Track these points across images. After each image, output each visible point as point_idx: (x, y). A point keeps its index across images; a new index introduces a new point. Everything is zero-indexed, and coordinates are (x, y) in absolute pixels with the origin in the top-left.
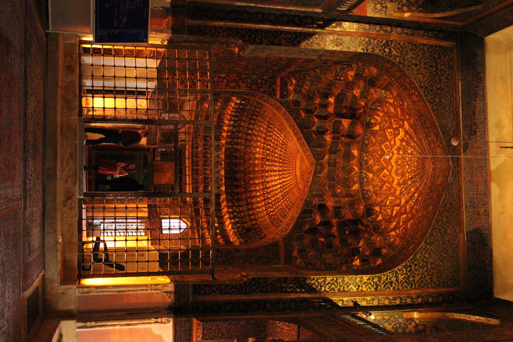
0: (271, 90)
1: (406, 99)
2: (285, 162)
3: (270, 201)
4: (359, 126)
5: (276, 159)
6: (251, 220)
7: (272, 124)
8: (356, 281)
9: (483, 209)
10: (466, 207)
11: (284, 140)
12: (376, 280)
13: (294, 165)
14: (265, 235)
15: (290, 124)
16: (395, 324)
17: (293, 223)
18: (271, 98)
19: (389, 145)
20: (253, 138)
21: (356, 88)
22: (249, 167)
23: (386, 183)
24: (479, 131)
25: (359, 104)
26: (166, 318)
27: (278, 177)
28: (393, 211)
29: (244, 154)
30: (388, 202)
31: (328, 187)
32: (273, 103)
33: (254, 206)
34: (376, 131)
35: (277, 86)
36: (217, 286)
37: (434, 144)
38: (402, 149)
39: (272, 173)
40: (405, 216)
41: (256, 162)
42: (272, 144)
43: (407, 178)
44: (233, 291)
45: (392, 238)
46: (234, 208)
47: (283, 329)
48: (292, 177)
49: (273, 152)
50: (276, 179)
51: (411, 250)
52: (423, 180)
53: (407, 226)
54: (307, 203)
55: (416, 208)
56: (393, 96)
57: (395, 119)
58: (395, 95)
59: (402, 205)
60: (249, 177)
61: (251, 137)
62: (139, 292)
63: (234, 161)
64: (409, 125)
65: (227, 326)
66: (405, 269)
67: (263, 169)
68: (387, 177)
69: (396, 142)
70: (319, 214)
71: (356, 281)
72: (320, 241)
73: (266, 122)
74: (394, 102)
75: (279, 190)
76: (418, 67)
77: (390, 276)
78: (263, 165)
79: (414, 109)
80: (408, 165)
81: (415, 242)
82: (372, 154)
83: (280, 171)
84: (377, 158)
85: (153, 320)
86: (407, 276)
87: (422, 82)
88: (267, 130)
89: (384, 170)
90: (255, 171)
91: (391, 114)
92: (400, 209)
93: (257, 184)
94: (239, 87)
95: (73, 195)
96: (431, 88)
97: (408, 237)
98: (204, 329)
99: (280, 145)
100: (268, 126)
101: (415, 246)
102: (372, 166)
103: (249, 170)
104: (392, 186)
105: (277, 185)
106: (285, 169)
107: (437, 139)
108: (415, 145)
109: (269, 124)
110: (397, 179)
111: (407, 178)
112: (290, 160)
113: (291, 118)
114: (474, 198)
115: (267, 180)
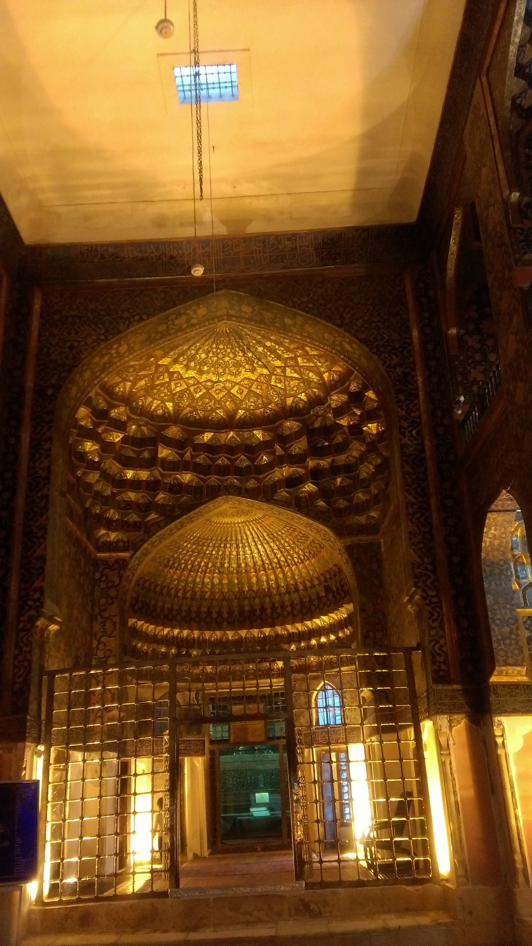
0: (116, 566)
1: (126, 362)
2: (224, 538)
3: (283, 559)
4: (168, 433)
5: (220, 553)
6: (313, 586)
7: (169, 561)
8: (406, 426)
9: (287, 242)
10: (284, 268)
11: (192, 541)
12: (402, 397)
13: (229, 525)
14: (335, 565)
15: (168, 534)
16: (469, 365)
17: (316, 524)
18: (130, 566)
19: (195, 387)
20: (189, 589)
21: (111, 438)
23: (252, 389)
24: (170, 251)
25: (136, 431)
26: (495, 728)
27: (247, 548)
28: (292, 378)
29: (214, 601)
30: (279, 385)
31: (259, 474)
32: (137, 562)
33: (291, 582)
34: (174, 407)
35: (111, 557)
36: (433, 643)
37: (192, 318)
38: (200, 367)
39: (242, 557)
40: (299, 359)
41: (225, 581)
42: (199, 560)
43: (243, 358)
44: (439, 616)
45: (333, 377)
46: (295, 612)
47: (494, 536)
48: (247, 528)
49: (209, 558)
50: (249, 552)
51: (352, 347)
52: (247, 334)
53: (314, 355)
54: (285, 504)
55: (288, 343)
56: (121, 382)
57: (156, 379)
58: (120, 380)
59: (283, 365)
60: (247, 592)
61: (187, 592)
62: (455, 776)
64: (164, 357)
65: (497, 625)
66: (384, 355)
67: (235, 571)
68: (243, 388)
69: (191, 376)
70: (301, 486)
71: (406, 426)
72: (342, 482)
73: (166, 570)
74: (130, 381)
75: (266, 546)
76: (76, 344)
77: (395, 377)
78: (229, 572)
79: (140, 349)
80: (223, 357)
81: (341, 342)
82: (208, 411)
83: (238, 547)
84: (214, 403)
85: (500, 751)
86: (394, 351)
87: (98, 338)
88: (177, 569)
89: (232, 394)
90: (238, 584)
91: (149, 384)
92: (289, 367)
94: (113, 616)
95: (302, 900)
96: (107, 324)
97: (332, 352)
98: (507, 664)
99: (199, 548)
100: (171, 568)
101: (345, 341)
102: (227, 411)
104: (256, 380)
105: (258, 549)
106: (234, 538)
107: (184, 314)
108: (193, 348)
109: (168, 565)
110: (245, 374)
111: (243, 358)
112: (220, 531)
113: (158, 534)
114: (270, 257)
115: (251, 564)
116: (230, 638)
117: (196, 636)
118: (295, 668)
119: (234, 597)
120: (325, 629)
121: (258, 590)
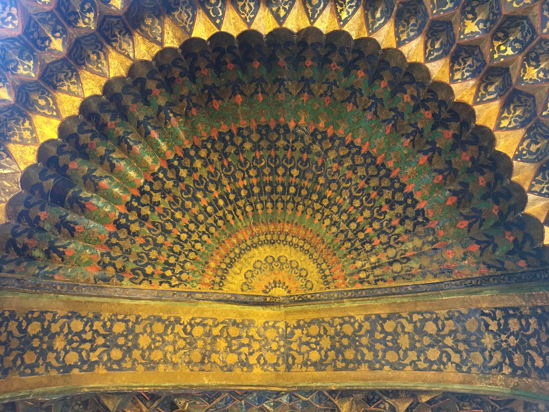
22: (287, 90)
29: (332, 81)
67: (282, 131)
119: (285, 83)
121: (234, 94)
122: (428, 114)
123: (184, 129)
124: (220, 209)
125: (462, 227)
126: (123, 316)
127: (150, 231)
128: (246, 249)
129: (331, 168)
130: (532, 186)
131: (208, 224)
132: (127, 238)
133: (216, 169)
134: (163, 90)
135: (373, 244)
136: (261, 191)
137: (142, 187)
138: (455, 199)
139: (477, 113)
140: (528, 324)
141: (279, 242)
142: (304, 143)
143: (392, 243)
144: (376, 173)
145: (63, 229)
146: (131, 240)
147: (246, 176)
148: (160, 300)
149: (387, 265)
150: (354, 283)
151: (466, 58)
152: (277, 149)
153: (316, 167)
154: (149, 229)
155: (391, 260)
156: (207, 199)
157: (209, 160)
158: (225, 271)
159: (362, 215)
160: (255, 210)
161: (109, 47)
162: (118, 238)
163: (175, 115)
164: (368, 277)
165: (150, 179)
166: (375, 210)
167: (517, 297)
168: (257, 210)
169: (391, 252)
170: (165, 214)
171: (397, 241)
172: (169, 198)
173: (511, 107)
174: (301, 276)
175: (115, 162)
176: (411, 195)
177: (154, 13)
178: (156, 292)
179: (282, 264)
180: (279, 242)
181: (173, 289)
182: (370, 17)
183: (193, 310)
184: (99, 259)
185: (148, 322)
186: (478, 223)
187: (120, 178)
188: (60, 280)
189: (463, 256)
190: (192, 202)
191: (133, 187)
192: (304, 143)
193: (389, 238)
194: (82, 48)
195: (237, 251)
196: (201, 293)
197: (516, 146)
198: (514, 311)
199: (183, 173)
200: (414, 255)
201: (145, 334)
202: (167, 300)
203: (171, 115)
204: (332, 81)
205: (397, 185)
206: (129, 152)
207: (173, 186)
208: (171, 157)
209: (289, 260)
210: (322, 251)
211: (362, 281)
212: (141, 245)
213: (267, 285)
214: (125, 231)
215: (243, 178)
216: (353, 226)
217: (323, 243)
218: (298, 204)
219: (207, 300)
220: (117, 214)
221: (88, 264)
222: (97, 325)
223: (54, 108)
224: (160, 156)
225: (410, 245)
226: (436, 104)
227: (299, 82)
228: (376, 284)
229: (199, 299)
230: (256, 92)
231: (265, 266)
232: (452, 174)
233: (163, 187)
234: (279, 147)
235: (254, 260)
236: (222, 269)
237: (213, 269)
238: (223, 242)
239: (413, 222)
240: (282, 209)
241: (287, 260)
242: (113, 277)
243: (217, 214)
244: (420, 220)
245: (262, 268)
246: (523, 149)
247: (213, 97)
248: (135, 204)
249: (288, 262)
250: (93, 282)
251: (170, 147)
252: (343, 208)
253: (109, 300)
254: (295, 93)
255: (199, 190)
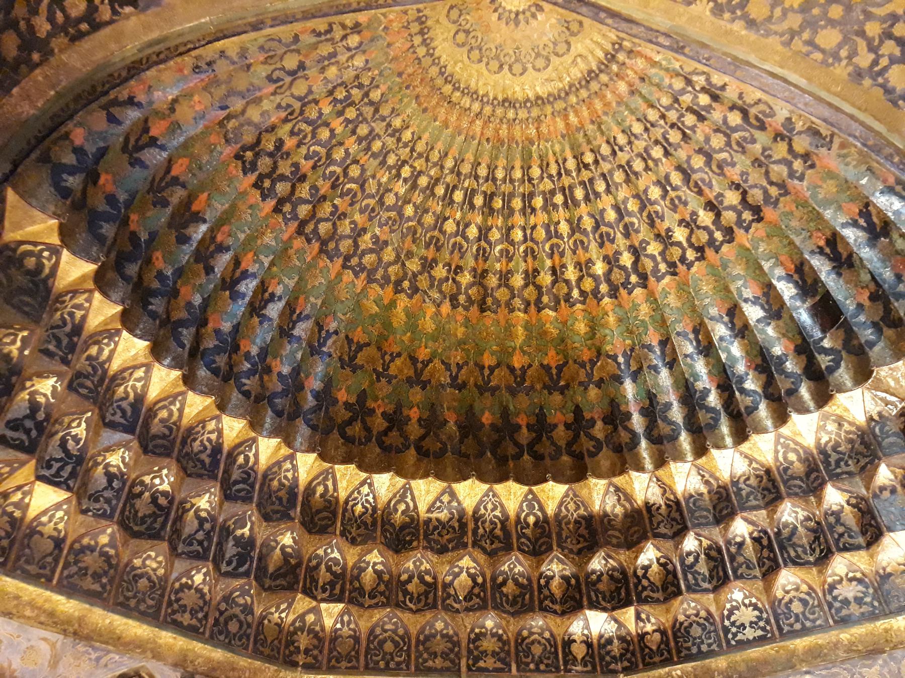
22: (448, 366)
61: (300, 318)
63: (414, 430)
93: (537, 333)
103: (459, 367)
116: (422, 508)
117: (304, 477)
118: (657, 636)
119: (449, 380)
120: (793, 478)
121: (524, 370)
122: (245, 346)
123: (607, 331)
124: (582, 183)
125: (180, 161)
126: (812, 56)
127: (710, 181)
128: (555, 99)
129: (392, 231)
130: (89, 300)
131: (610, 162)
132: (751, 187)
133: (574, 253)
134: (623, 408)
135: (331, 99)
136: (509, 201)
137: (697, 259)
138: (195, 208)
139: (181, 382)
140: (51, 19)
141: (496, 102)
142: (431, 276)
143: (297, 105)
144: (320, 226)
145: (844, 256)
146: (746, 181)
147: (528, 232)
148: (735, 58)
149: (308, 63)
150: (370, 22)
151: (201, 452)
152: (474, 270)
153: (415, 233)
154: (711, 187)
155: (300, 74)
156: (601, 207)
157: (581, 270)
158: (603, 67)
159: (347, 151)
160: (526, 168)
161: (680, 496)
162: (766, 192)
163: (614, 358)
164: (345, 37)
165: (681, 268)
166: (323, 160)
167: (78, 65)
168: (522, 167)
169: (300, 88)
170: (677, 202)
171: (289, 110)
172: (662, 226)
173: (132, 395)
174: (467, 32)
175: (726, 319)
176: (264, 197)
177: (610, 521)
178: (738, 73)
179: (497, 57)
180: (496, 102)
181: (706, 69)
182: (331, 487)
183: (684, 19)
184: (810, 171)
185: (773, 27)
186: (157, 180)
187: (727, 289)
188: (888, 170)
189: (177, 106)
190: (626, 208)
191: (712, 266)
192: (431, 276)
193: (302, 112)
194: (714, 508)
195: (573, 99)
196: (658, 44)
197: (120, 348)
198: (79, 31)
199: (627, 259)
200: (260, 89)
201: (787, 5)
202: (725, 54)
203: (621, 359)
204: (383, 380)
205: (287, 208)
206: (700, 324)
207: (648, 244)
208: (638, 291)
209: (483, 64)
210: (422, 80)
211: (357, 28)
212: (733, 165)
213: (531, 20)
214: (750, 200)
215: (534, 228)
216: (363, 130)
217: (417, 97)
218: (452, 171)
219: (652, 30)
220: (752, 230)
221: (831, 175)
222: (865, 59)
223: (779, 447)
224: (656, 300)
225: (266, 105)
226: (235, 370)
227: (429, 381)
228: (330, 25)
229: (667, 35)
230: (492, 369)
231: (528, 57)
232: (202, 250)
233: (666, 248)
234: (470, 273)
235: (545, 74)
236: (608, 74)
237: (623, 79)
238: (593, 122)
239: (261, 147)
240: (479, 164)
241: (487, 64)
242: (800, 133)
243: (590, 175)
244: (249, 154)
245: (533, 55)
246: (108, 345)
247: (554, 371)
248: (718, 235)
249: (485, 60)
250: (835, 138)
251: (636, 307)
252: (377, 161)
253: (824, 94)
254: (437, 363)
255: (609, 225)
